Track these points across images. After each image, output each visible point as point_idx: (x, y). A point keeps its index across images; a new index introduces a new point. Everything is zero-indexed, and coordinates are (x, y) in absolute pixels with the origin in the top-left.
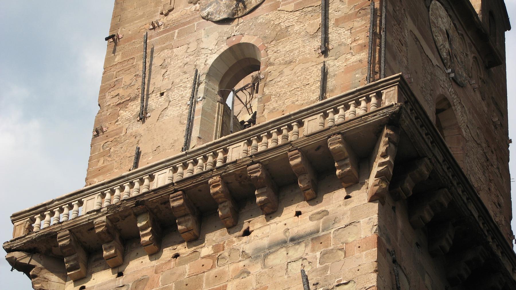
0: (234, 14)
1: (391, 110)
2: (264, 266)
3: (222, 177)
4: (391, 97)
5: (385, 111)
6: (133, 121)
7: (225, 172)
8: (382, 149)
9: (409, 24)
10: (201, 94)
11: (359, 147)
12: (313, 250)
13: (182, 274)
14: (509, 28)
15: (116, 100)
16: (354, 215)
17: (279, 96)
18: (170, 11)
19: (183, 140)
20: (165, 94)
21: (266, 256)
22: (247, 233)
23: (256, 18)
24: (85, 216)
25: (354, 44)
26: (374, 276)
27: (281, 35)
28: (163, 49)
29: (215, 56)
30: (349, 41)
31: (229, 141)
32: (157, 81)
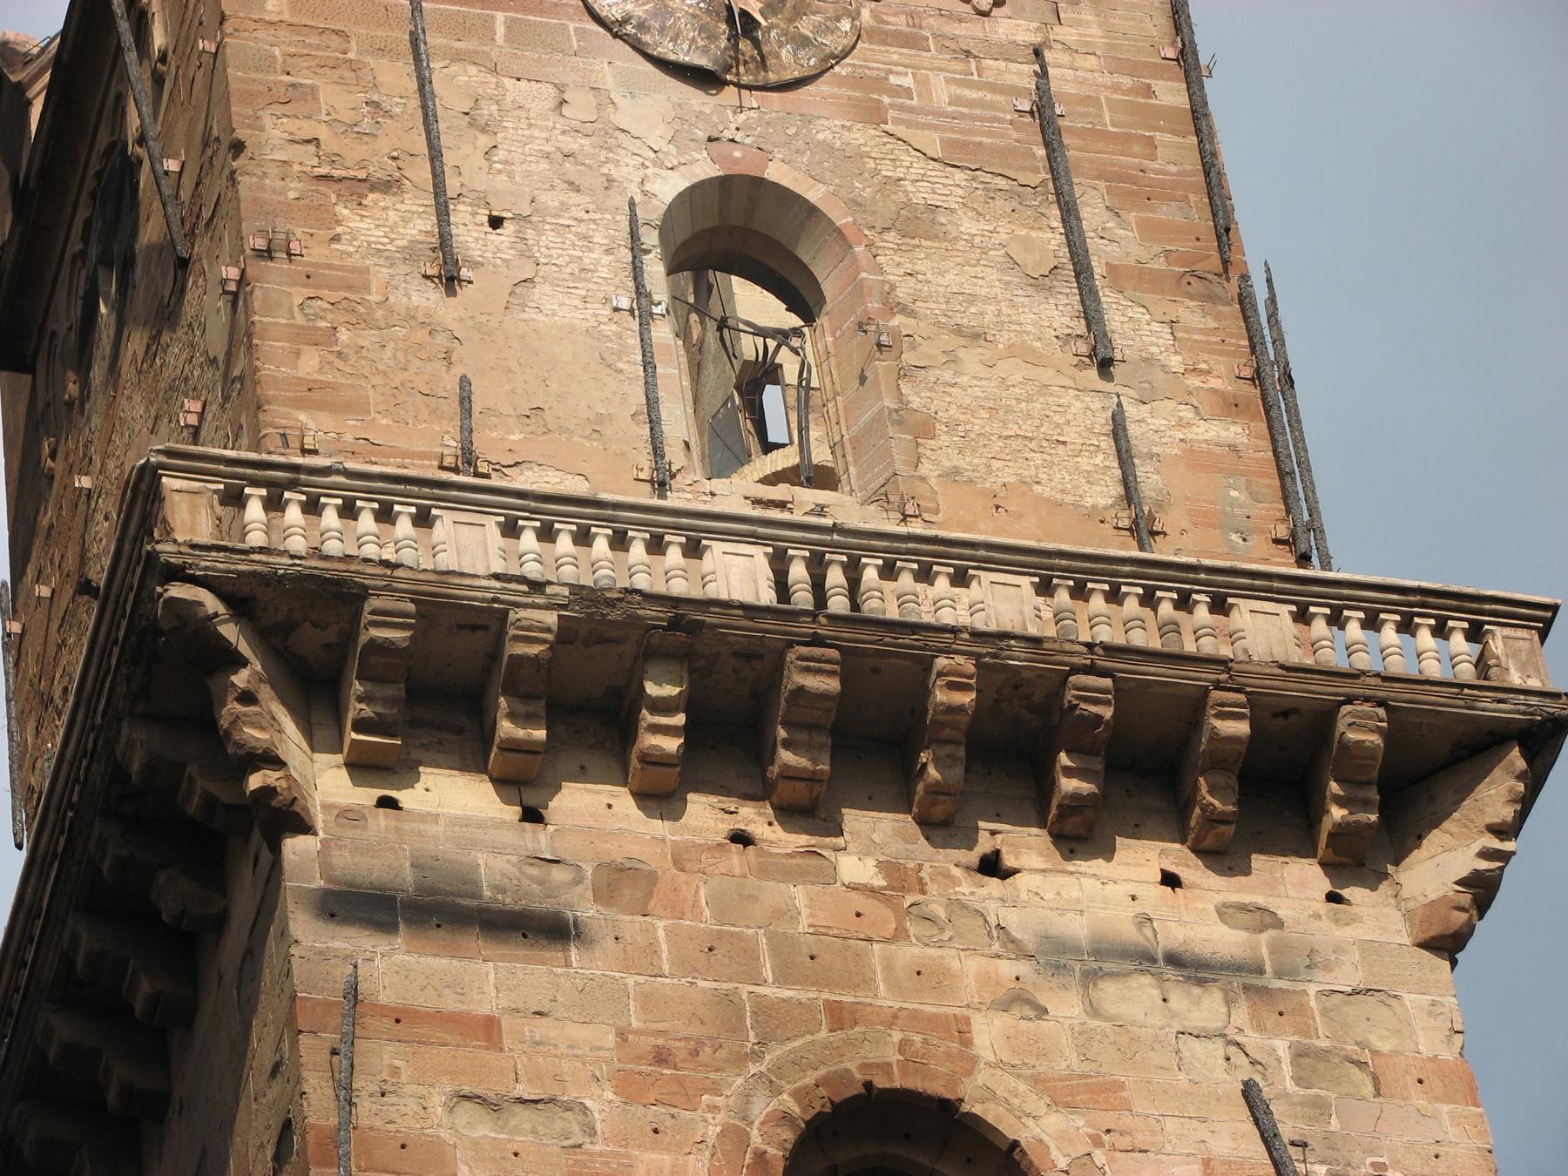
0: (728, 69)
2: (1094, 1010)
5: (1534, 700)
7: (994, 656)
21: (1091, 977)
22: (991, 866)
23: (808, 120)
24: (484, 583)
25: (1194, 382)
31: (982, 553)
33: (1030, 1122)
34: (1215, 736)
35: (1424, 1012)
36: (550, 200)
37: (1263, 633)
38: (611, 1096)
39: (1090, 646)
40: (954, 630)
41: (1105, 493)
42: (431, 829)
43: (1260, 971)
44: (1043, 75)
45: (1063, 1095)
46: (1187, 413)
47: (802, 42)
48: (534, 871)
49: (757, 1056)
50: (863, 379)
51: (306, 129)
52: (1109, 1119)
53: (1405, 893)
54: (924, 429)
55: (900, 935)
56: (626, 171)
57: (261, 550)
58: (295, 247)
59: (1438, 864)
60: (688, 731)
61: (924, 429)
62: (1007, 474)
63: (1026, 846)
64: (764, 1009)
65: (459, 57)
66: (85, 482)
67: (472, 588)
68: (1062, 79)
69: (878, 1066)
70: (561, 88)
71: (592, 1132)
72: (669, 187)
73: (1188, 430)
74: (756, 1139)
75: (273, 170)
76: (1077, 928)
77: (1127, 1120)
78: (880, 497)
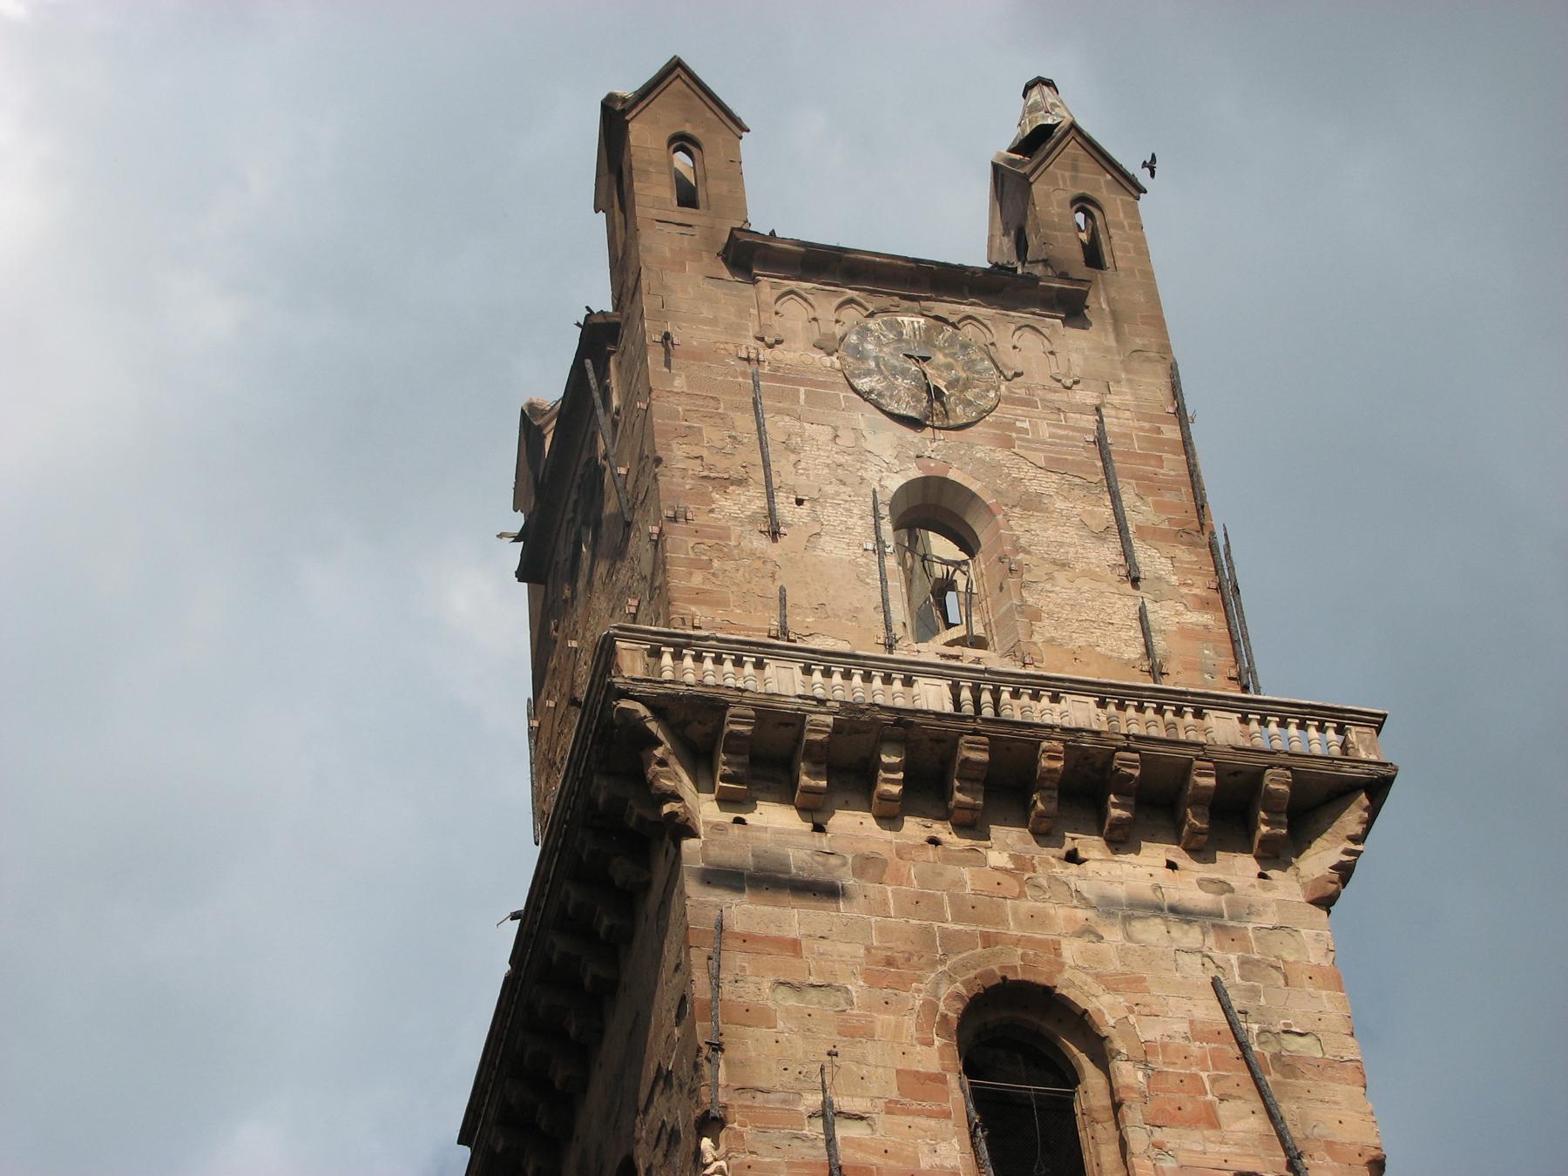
0: (927, 418)
2: (1129, 937)
5: (1373, 767)
21: (1127, 919)
22: (1073, 857)
23: (971, 446)
25: (1184, 590)
34: (1196, 786)
35: (1313, 938)
36: (829, 490)
37: (1223, 729)
39: (1127, 736)
40: (1052, 727)
41: (1135, 651)
42: (763, 835)
43: (1222, 916)
44: (1101, 421)
46: (1181, 608)
47: (969, 403)
48: (820, 859)
49: (942, 962)
50: (1001, 589)
51: (696, 451)
52: (1138, 998)
53: (1302, 873)
54: (1035, 615)
55: (1021, 895)
56: (871, 474)
57: (670, 682)
58: (689, 516)
59: (1320, 858)
60: (904, 782)
61: (1035, 615)
62: (1082, 642)
63: (1091, 846)
64: (947, 936)
65: (779, 412)
66: (574, 644)
70: (835, 429)
72: (895, 483)
73: (1181, 617)
74: (942, 1008)
75: (678, 474)
76: (1120, 892)
77: (1148, 999)
78: (1012, 653)
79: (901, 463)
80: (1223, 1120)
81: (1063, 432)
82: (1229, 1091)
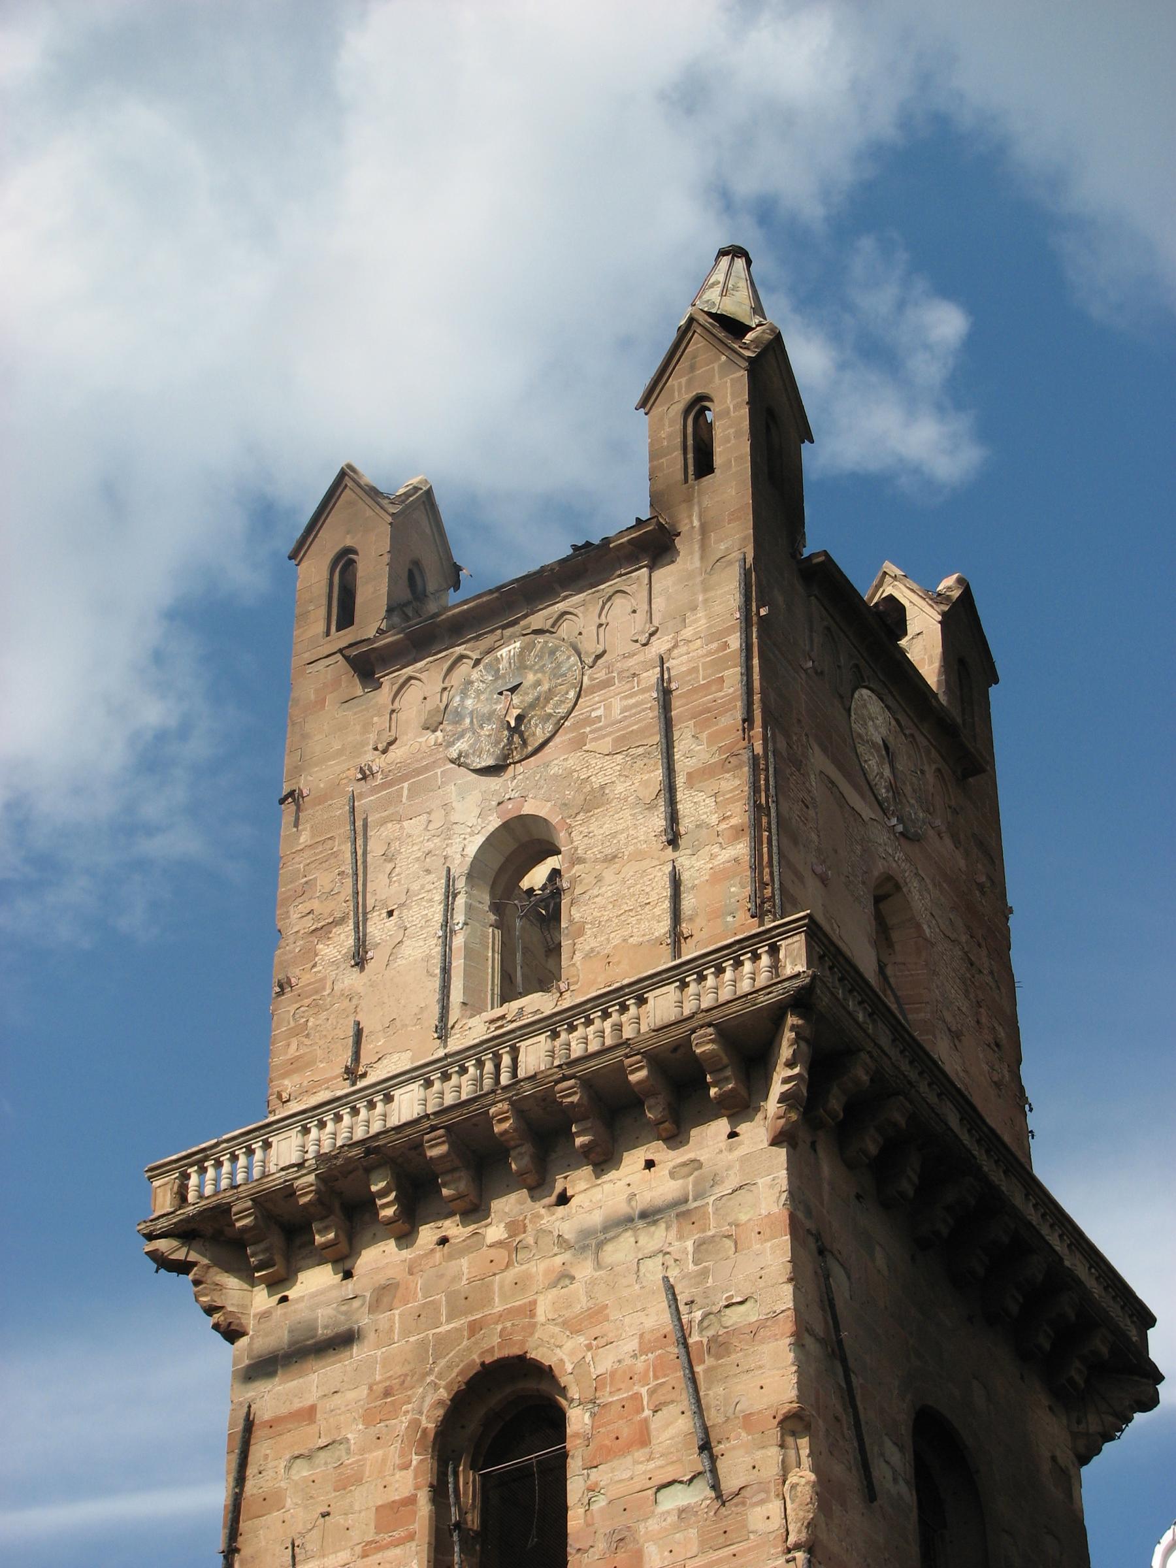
0: (506, 757)
1: (797, 983)
2: (599, 1265)
3: (512, 1104)
4: (794, 959)
5: (786, 984)
6: (343, 966)
7: (516, 1095)
8: (786, 1052)
9: (818, 760)
10: (459, 917)
11: (747, 1043)
12: (681, 1237)
13: (457, 1278)
14: (996, 681)
15: (309, 924)
16: (744, 1166)
17: (598, 924)
18: (390, 744)
19: (436, 1009)
20: (395, 913)
21: (600, 1245)
22: (563, 1199)
23: (547, 765)
24: (278, 1175)
25: (723, 826)
26: (788, 1289)
27: (594, 801)
28: (383, 822)
29: (480, 840)
30: (714, 819)
32: (380, 888)
33: (558, 1351)
38: (361, 1427)
42: (302, 1305)
45: (573, 1327)
46: (716, 849)
48: (344, 1308)
67: (274, 1180)
68: (677, 665)
69: (487, 1351)
71: (348, 1451)
79: (484, 820)
80: (653, 1433)
81: (632, 701)
82: (662, 1399)
